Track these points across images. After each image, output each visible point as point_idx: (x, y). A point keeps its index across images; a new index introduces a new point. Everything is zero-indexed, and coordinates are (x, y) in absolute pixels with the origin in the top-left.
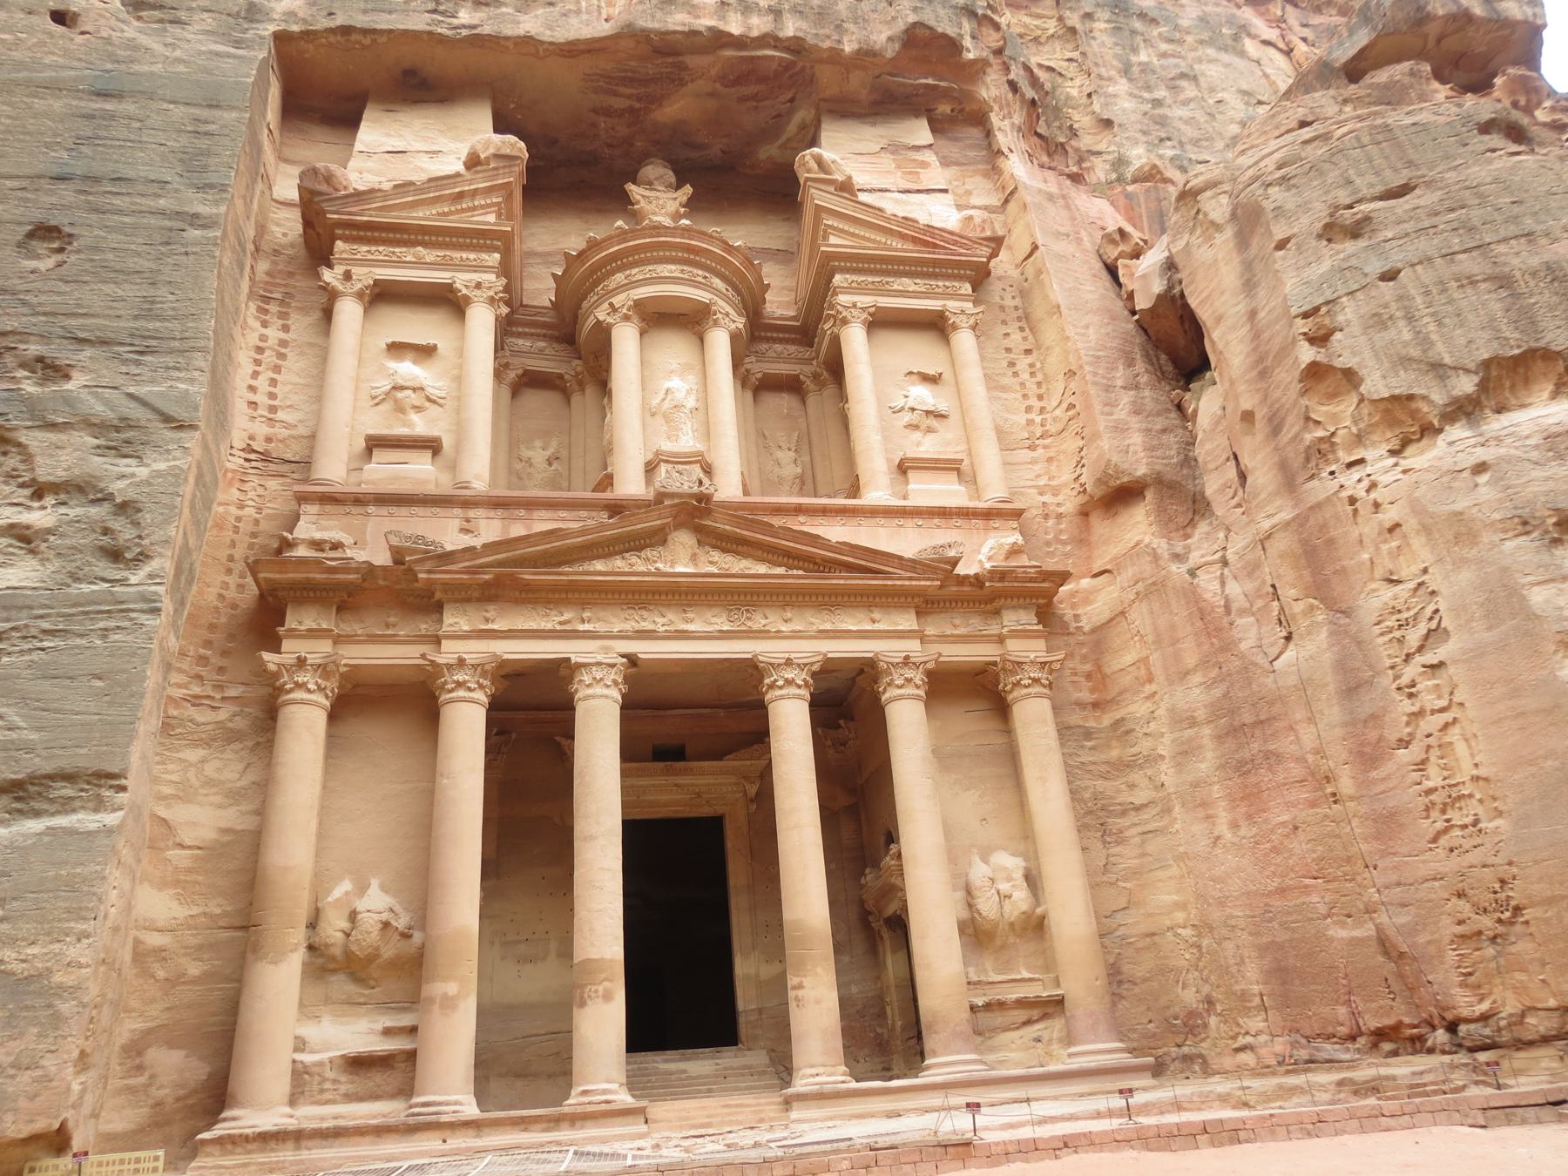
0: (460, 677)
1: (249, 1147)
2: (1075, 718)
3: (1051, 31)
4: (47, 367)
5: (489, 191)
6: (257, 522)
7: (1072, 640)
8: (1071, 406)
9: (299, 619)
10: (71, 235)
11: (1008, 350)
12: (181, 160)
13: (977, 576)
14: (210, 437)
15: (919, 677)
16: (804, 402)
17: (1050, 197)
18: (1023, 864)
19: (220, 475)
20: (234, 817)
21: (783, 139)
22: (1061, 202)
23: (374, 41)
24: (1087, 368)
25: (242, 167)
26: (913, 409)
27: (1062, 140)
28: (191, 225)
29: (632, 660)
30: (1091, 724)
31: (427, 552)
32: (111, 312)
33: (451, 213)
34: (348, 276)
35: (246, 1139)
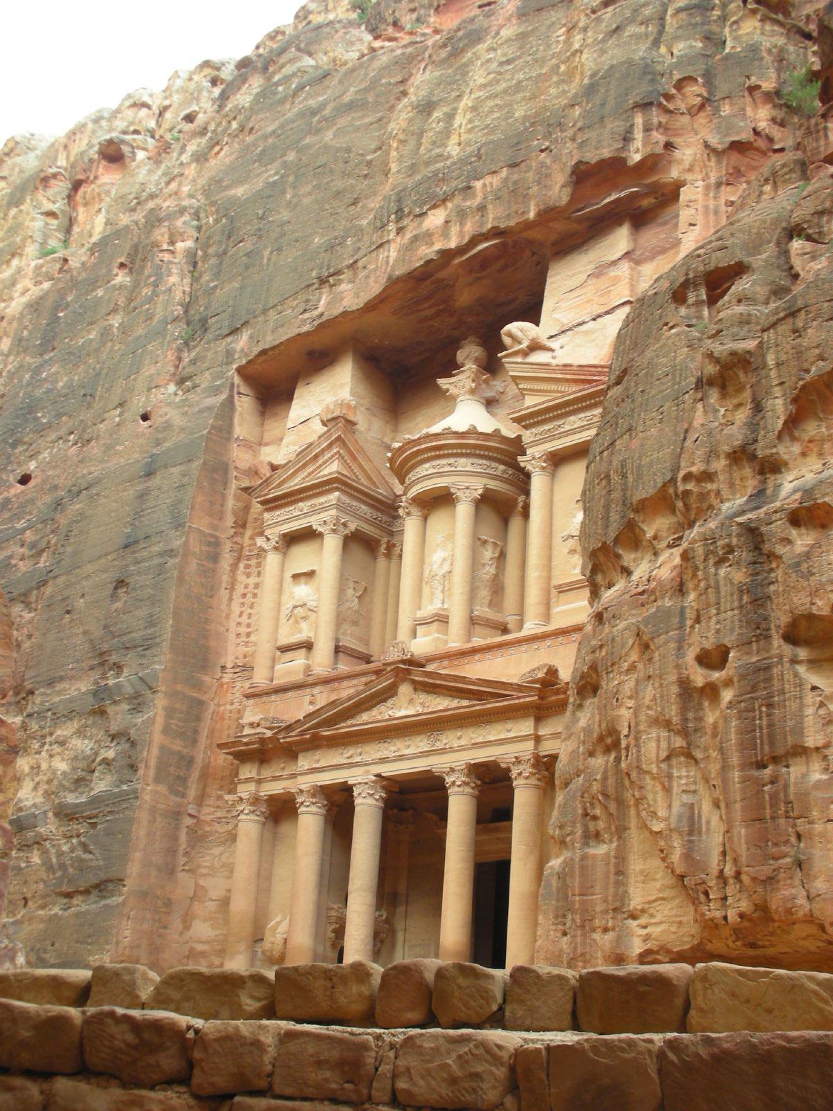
4: (118, 667)
5: (330, 446)
6: (239, 711)
15: (527, 770)
19: (204, 698)
29: (378, 775)
33: (315, 470)
34: (268, 539)
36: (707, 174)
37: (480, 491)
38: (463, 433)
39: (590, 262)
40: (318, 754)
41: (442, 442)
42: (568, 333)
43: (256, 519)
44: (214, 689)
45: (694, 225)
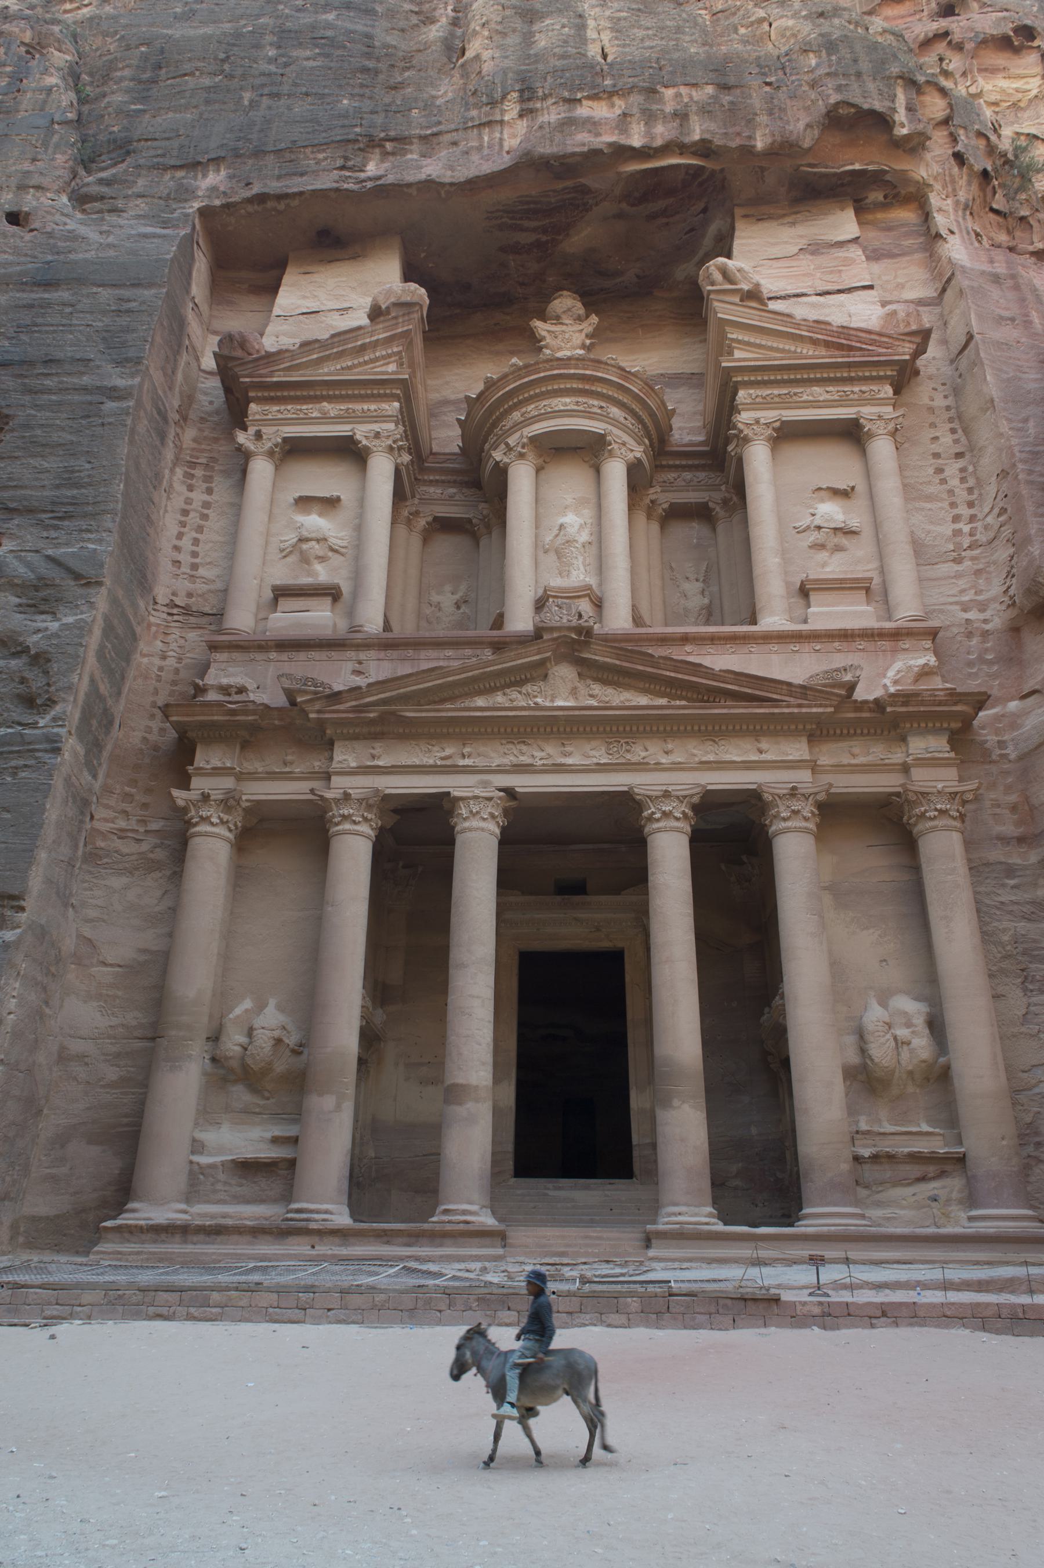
0: (346, 812)
1: (143, 1237)
2: (996, 854)
3: (1034, 92)
5: (389, 340)
6: (177, 671)
7: (994, 769)
8: (1003, 511)
9: (206, 758)
10: (7, 416)
11: (936, 456)
12: (104, 339)
13: (876, 701)
14: (120, 593)
15: (808, 809)
16: (714, 529)
17: (996, 279)
18: (928, 1010)
19: (138, 630)
20: (150, 938)
21: (701, 253)
22: (1010, 283)
23: (288, 205)
24: (1020, 466)
25: (158, 339)
26: (819, 528)
27: (1023, 213)
28: (111, 398)
29: (510, 793)
30: (1016, 860)
31: (316, 693)
32: (36, 483)
33: (354, 366)
34: (259, 435)
35: (141, 1229)
36: (954, 190)
37: (638, 455)
38: (629, 372)
39: (801, 237)
40: (378, 747)
41: (600, 374)
42: (780, 301)
43: (202, 418)
44: (145, 625)
45: (952, 232)
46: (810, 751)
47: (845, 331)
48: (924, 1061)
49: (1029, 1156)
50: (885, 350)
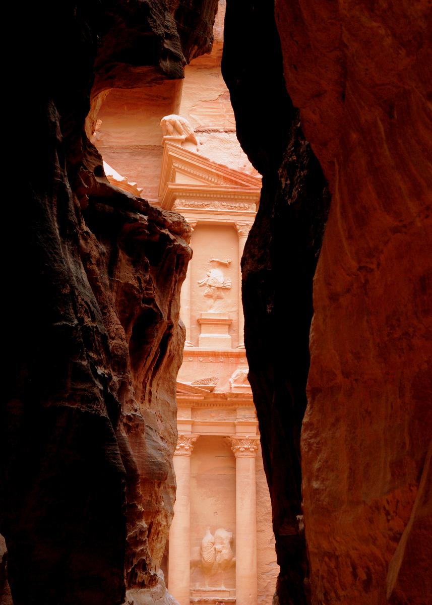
13: (224, 394)
15: (187, 445)
26: (210, 286)
42: (204, 133)
46: (192, 414)
47: (234, 173)
48: (225, 560)
49: (263, 600)
50: (254, 187)
